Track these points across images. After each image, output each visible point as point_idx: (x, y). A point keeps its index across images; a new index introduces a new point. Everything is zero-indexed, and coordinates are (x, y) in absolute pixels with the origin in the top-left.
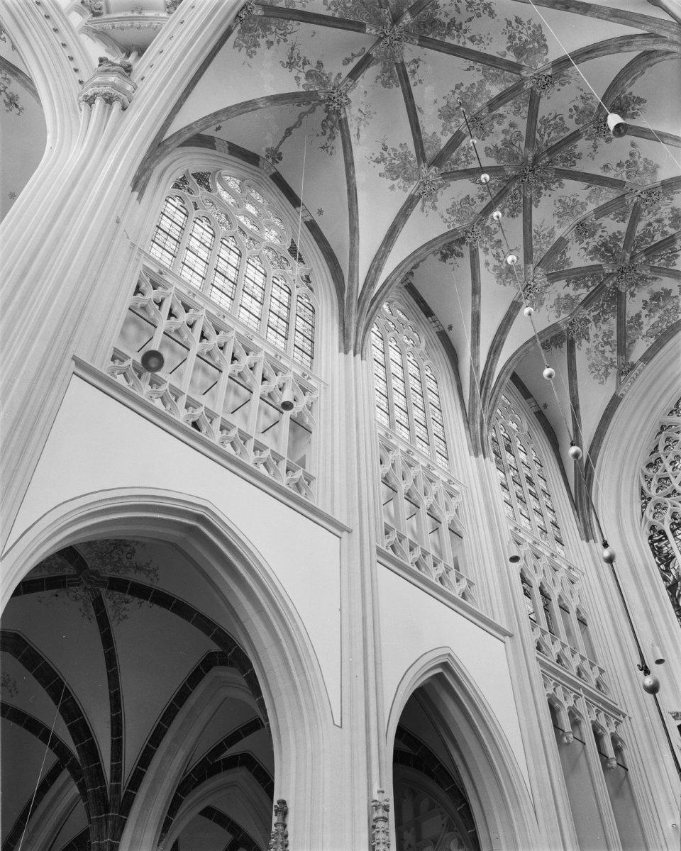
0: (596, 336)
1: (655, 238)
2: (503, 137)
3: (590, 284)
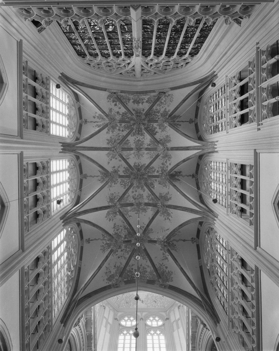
0: (163, 107)
1: (124, 125)
2: (138, 190)
3: (151, 125)
